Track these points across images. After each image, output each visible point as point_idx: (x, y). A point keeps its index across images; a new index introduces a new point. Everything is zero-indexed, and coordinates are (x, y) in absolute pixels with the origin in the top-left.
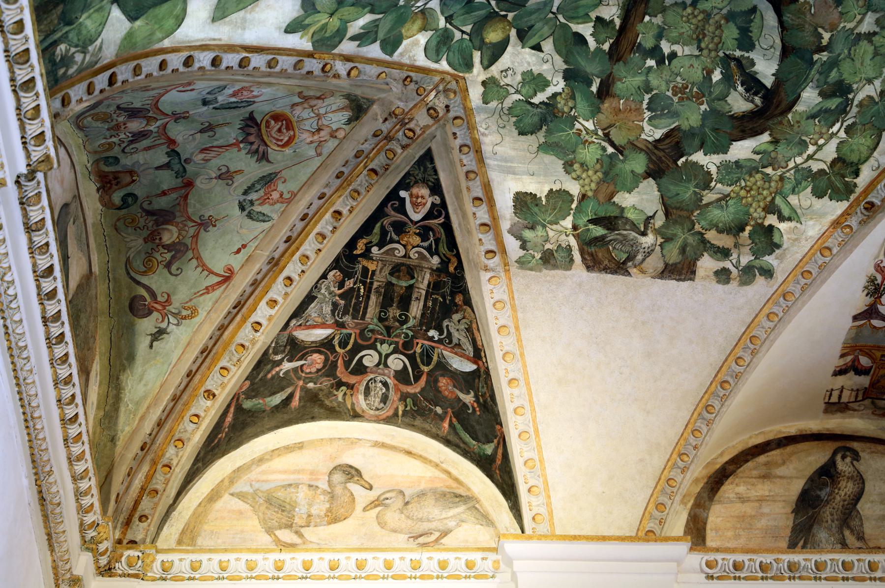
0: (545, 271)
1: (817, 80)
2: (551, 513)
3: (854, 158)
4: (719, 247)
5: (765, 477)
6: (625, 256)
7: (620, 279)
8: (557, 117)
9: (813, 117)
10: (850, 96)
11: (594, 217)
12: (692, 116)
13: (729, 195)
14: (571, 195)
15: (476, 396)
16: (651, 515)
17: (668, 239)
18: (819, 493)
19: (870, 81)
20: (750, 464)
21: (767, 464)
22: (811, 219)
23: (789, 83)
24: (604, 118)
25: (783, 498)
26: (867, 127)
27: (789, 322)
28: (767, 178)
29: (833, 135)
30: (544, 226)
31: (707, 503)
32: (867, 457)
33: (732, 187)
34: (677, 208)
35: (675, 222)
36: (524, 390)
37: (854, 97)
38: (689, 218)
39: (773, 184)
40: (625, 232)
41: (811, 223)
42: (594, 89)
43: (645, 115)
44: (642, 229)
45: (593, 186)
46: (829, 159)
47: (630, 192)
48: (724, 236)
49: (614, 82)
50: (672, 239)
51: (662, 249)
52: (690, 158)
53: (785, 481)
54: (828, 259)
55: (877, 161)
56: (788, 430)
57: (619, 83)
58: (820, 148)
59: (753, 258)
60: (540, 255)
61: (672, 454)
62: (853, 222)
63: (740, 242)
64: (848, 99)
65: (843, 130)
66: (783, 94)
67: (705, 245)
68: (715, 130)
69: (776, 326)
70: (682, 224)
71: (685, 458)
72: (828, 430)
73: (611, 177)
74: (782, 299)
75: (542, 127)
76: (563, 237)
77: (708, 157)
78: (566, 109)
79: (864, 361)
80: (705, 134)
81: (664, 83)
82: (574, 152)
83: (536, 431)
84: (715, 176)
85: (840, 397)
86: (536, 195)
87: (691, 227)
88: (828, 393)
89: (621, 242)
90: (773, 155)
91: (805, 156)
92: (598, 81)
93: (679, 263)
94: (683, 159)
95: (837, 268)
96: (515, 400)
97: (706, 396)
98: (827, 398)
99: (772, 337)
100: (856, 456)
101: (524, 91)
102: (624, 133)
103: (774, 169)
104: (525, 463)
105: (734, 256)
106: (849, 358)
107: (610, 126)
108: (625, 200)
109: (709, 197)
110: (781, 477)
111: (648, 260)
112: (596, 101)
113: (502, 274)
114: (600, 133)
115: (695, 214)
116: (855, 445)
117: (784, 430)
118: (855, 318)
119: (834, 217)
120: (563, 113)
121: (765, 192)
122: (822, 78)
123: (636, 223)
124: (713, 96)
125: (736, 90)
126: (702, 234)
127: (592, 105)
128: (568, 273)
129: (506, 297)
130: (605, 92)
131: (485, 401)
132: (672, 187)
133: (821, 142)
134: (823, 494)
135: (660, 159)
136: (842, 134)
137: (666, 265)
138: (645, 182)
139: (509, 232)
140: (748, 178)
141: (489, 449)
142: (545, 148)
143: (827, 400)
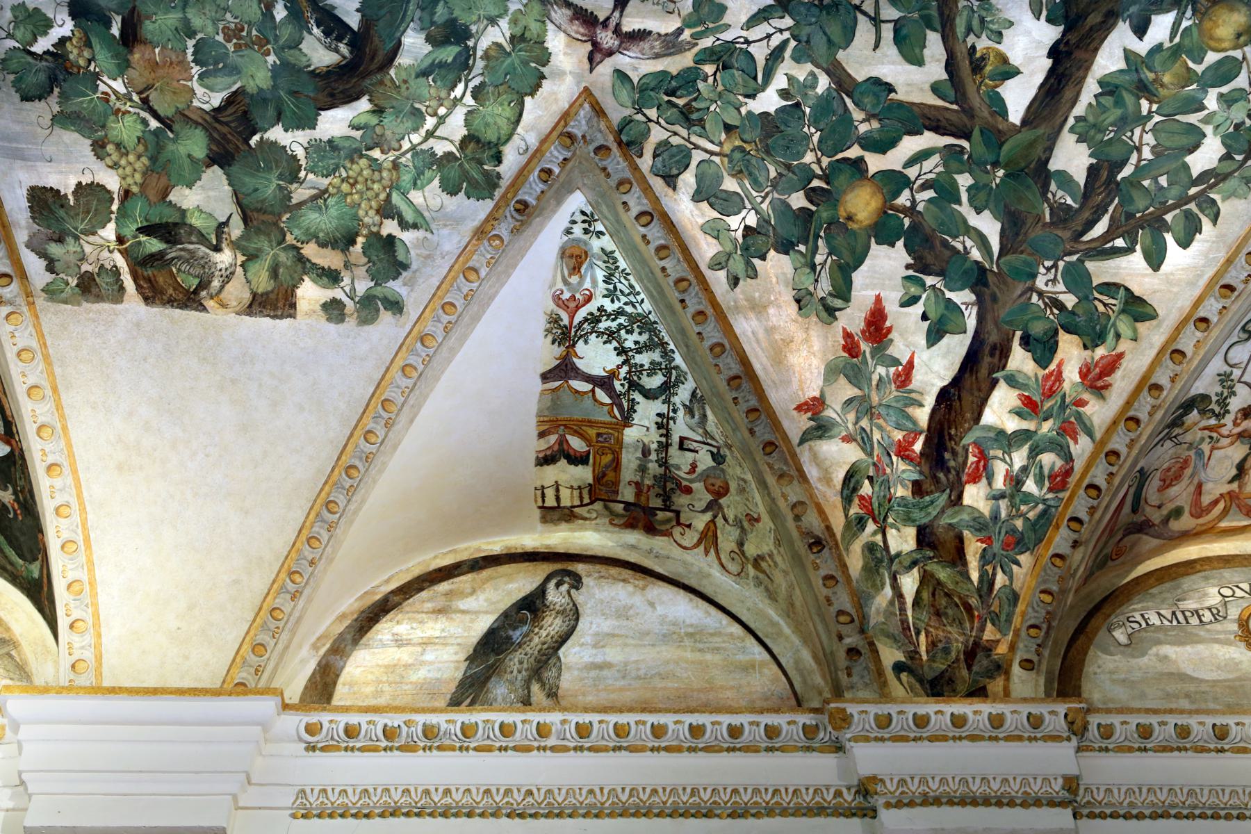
0: (85, 304)
1: (420, 19)
2: (99, 658)
3: (491, 135)
4: (323, 268)
5: (440, 611)
6: (195, 282)
7: (192, 315)
8: (71, 74)
9: (424, 74)
10: (471, 43)
11: (145, 224)
12: (258, 73)
13: (326, 191)
14: (109, 192)
15: (15, 493)
16: (244, 661)
17: (252, 257)
18: (511, 633)
19: (493, 21)
20: (424, 594)
21: (449, 594)
22: (445, 226)
23: (381, 23)
24: (138, 74)
25: (459, 641)
26: (501, 89)
27: (437, 379)
28: (375, 165)
29: (457, 102)
30: (77, 238)
31: (349, 647)
32: (592, 583)
33: (330, 178)
34: (259, 210)
35: (259, 231)
36: (69, 480)
37: (476, 44)
38: (276, 224)
39: (385, 174)
40: (191, 247)
41: (445, 231)
42: (115, 30)
43: (193, 71)
44: (214, 242)
45: (138, 177)
46: (458, 137)
47: (190, 185)
48: (327, 251)
49: (140, 22)
50: (257, 257)
51: (245, 271)
52: (266, 136)
53: (468, 617)
54: (476, 284)
55: (523, 139)
56: (490, 547)
57: (147, 22)
58: (442, 120)
59: (372, 284)
60: (75, 282)
61: (279, 572)
62: (503, 230)
63: (352, 259)
64: (467, 47)
65: (468, 94)
66: (376, 40)
67: (304, 265)
68: (294, 93)
69: (415, 384)
70: (268, 235)
71: (297, 578)
72: (547, 546)
73: (161, 169)
74: (419, 344)
75: (52, 91)
76: (105, 254)
77: (289, 133)
78: (82, 62)
79: (576, 444)
80: (280, 98)
81: (209, 23)
82: (103, 127)
83: (87, 540)
84: (303, 162)
85: (558, 498)
86: (58, 191)
87: (280, 238)
88: (539, 493)
89: (187, 261)
90: (378, 130)
91: (423, 132)
92: (119, 19)
93: (272, 291)
94: (256, 138)
95: (492, 298)
96: (57, 495)
97: (327, 488)
98: (540, 500)
99: (411, 401)
100: (577, 582)
101: (19, 34)
102: (168, 98)
103: (383, 152)
104: (69, 586)
105: (346, 281)
106: (553, 439)
107: (148, 88)
108: (187, 198)
109: (300, 194)
110: (463, 612)
111: (228, 287)
112: (121, 48)
113: (25, 309)
114: (135, 97)
115: (284, 219)
116: (580, 568)
117: (484, 547)
118: (545, 377)
119: (476, 223)
120: (79, 67)
121: (376, 186)
122: (426, 16)
123: (204, 232)
124: (281, 42)
125: (311, 34)
126: (298, 249)
127: (116, 56)
128: (119, 307)
129: (34, 344)
130: (131, 36)
131: (25, 499)
132: (247, 180)
133: (442, 111)
134: (516, 635)
135: (224, 136)
136: (469, 100)
137: (254, 295)
138: (209, 171)
139: (27, 246)
140: (349, 165)
141: (35, 570)
142: (63, 119)
143: (540, 504)
